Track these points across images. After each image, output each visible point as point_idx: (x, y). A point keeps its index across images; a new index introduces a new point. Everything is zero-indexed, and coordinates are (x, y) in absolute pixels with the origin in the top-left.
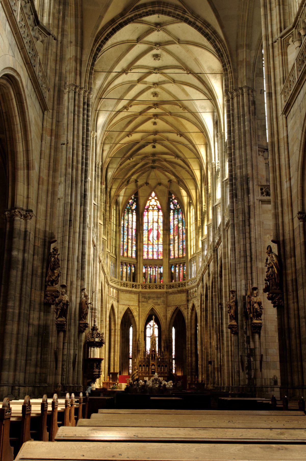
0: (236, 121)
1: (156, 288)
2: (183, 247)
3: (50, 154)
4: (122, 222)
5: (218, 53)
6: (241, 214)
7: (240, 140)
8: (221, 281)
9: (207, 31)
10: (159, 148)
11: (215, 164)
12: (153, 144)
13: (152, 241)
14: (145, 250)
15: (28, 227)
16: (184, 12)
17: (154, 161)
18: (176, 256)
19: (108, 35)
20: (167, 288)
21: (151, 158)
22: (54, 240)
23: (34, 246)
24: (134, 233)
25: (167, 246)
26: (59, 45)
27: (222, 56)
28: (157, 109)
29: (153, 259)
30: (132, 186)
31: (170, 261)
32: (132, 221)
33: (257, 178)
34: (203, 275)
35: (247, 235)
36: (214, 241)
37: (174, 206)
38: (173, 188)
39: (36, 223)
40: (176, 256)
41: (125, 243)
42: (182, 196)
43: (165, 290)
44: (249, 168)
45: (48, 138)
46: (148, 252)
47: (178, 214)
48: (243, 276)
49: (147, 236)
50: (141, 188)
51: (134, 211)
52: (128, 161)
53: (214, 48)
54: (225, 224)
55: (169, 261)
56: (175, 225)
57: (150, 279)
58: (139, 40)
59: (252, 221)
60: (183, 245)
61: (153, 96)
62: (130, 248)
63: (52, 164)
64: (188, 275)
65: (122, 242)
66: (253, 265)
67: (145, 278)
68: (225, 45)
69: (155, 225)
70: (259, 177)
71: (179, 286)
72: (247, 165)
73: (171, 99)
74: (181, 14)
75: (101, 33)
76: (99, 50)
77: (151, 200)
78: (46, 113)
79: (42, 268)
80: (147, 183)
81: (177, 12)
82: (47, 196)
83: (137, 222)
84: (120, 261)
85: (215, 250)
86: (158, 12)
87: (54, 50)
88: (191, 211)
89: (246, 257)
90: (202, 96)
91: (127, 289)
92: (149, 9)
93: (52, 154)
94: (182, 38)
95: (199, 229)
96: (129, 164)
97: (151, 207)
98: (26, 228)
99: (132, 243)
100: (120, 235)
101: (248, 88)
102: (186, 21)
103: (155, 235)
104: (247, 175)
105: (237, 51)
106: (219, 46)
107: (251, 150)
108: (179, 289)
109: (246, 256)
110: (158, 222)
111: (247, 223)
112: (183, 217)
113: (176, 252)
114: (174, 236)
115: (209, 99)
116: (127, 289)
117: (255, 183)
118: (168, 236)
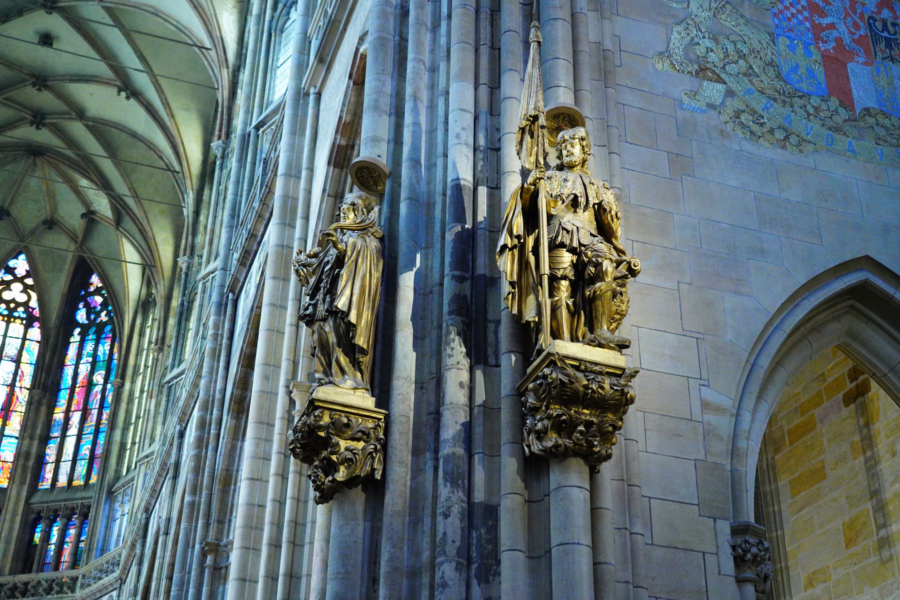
2: (93, 451)
8: (238, 434)
17: (39, 118)
18: (63, 480)
25: (36, 442)
31: (35, 499)
37: (88, 315)
38: (99, 245)
40: (63, 480)
47: (97, 342)
55: (29, 497)
56: (80, 378)
60: (94, 443)
88: (148, 331)
110: (17, 361)
112: (115, 350)
113: (65, 468)
114: (68, 412)
118: (43, 410)
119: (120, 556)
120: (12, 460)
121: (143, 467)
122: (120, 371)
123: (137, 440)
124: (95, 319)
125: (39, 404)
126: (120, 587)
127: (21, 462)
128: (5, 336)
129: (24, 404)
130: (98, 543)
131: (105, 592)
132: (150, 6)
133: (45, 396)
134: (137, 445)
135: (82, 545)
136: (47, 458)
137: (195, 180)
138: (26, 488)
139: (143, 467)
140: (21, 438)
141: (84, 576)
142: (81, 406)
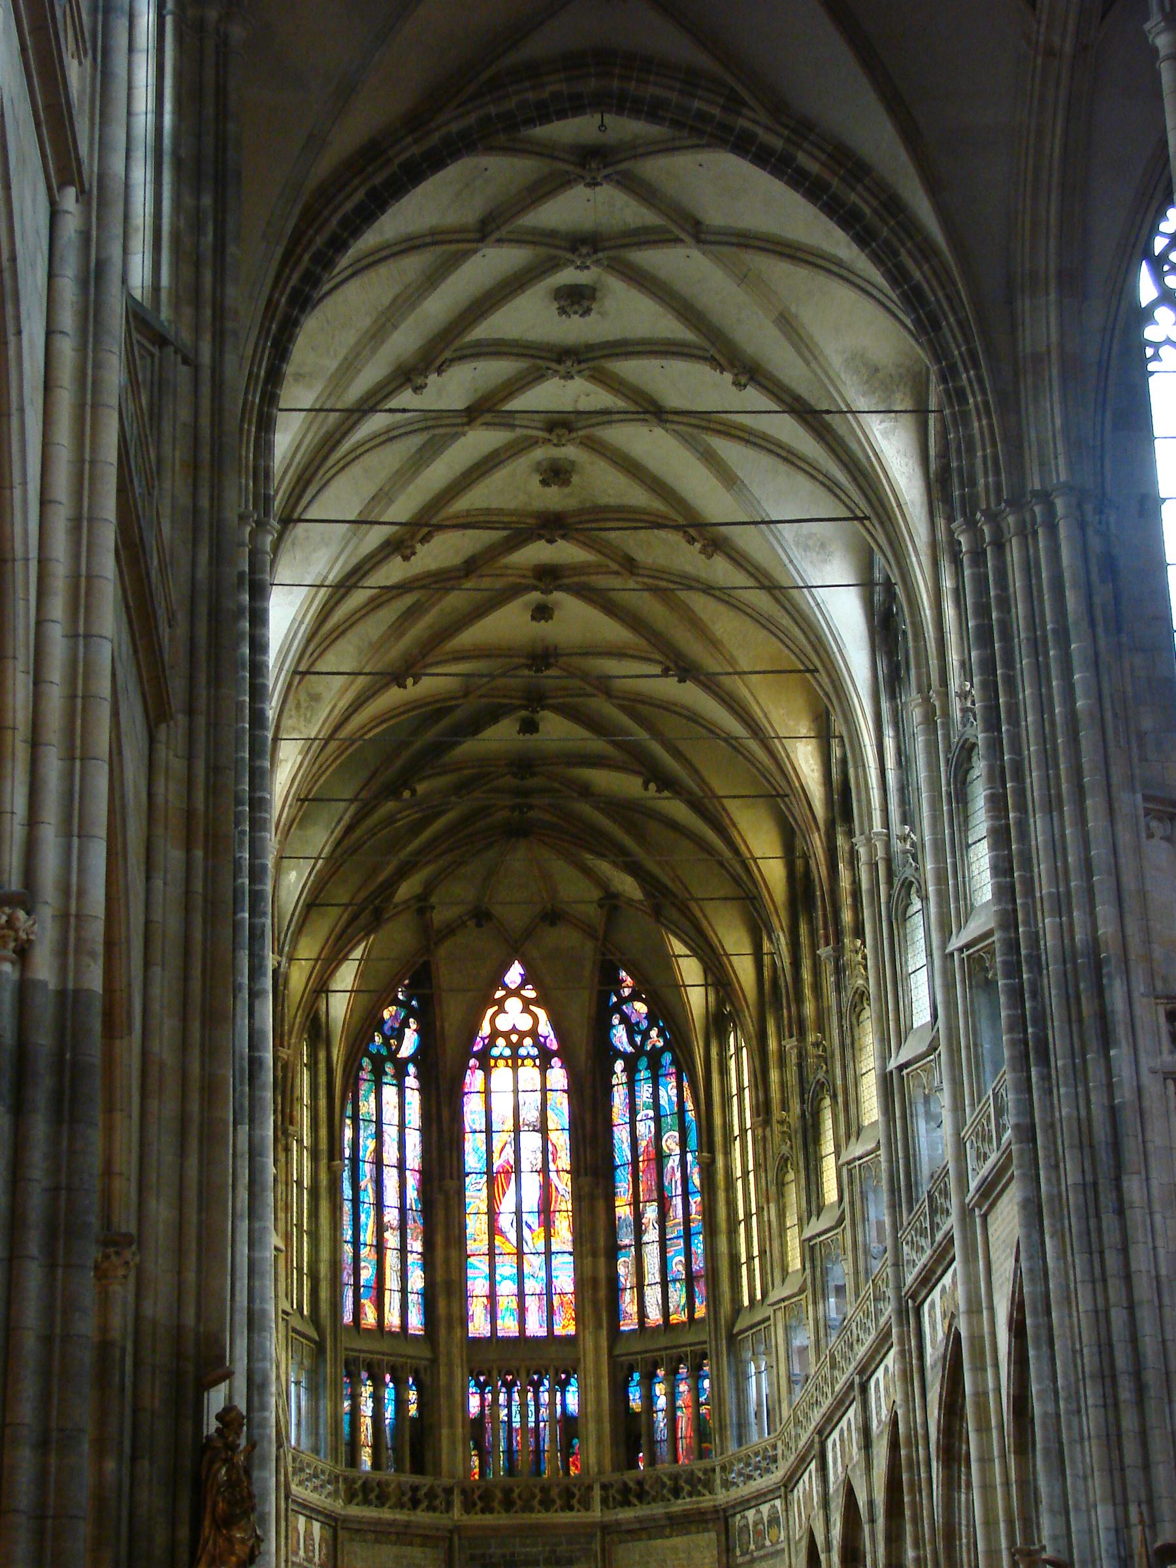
0: (1024, 662)
1: (547, 1504)
2: (688, 1265)
3: (187, 940)
4: (348, 1133)
5: (915, 310)
6: (1076, 1151)
7: (1049, 760)
9: (853, 197)
10: (556, 730)
11: (888, 845)
12: (523, 713)
13: (512, 1235)
14: (478, 1285)
15: (116, 1321)
16: (734, 103)
18: (654, 1315)
19: (345, 223)
20: (604, 1501)
21: (508, 781)
22: (220, 1371)
23: (135, 1411)
24: (412, 1194)
25: (602, 1260)
26: (206, 390)
27: (936, 327)
28: (560, 541)
29: (522, 1338)
30: (398, 936)
32: (402, 1126)
33: (1149, 958)
34: (823, 1432)
35: (1112, 1261)
36: (897, 1264)
39: (138, 1295)
40: (654, 1315)
41: (364, 1251)
42: (678, 987)
43: (596, 1514)
44: (1105, 910)
45: (175, 855)
46: (492, 1297)
48: (1098, 1485)
49: (484, 1208)
50: (448, 944)
51: (412, 1069)
52: (391, 805)
53: (894, 282)
54: (973, 1185)
57: (509, 1451)
58: (486, 229)
59: (1133, 1187)
61: (545, 483)
62: (392, 1281)
63: (196, 986)
64: (722, 1428)
65: (348, 1249)
66: (1152, 1419)
67: (479, 1446)
68: (947, 272)
69: (531, 1142)
70: (1158, 952)
71: (676, 1492)
72: (1090, 891)
73: (639, 497)
74: (716, 111)
75: (310, 217)
76: (303, 300)
77: (501, 1003)
78: (162, 732)
79: (173, 1524)
80: (481, 916)
81: (697, 104)
82: (182, 1154)
83: (424, 1130)
84: (342, 1355)
85: (910, 1309)
86: (601, 102)
87: (185, 414)
88: (732, 1064)
89: (1114, 1378)
90: (829, 507)
91: (386, 1514)
92: (555, 85)
93: (198, 936)
94: (715, 216)
95: (782, 1170)
96: (391, 819)
97: (501, 1042)
98: (104, 1329)
99: (403, 1251)
100: (336, 1209)
101: (1079, 496)
102: (744, 145)
103: (531, 1200)
104: (1095, 943)
105: (1010, 302)
106: (917, 275)
107: (1111, 811)
108: (680, 1505)
109: (1107, 1376)
111: (1107, 1199)
112: (687, 1093)
113: (653, 1295)
114: (635, 1202)
115: (856, 518)
116: (386, 1514)
117: (1140, 988)
118: (601, 1205)
119: (775, 1447)
120: (571, 1289)
121: (780, 1314)
122: (704, 1139)
123: (756, 1253)
124: (643, 1042)
125: (592, 1197)
126: (786, 1497)
127: (588, 1294)
128: (516, 1091)
129: (568, 1197)
130: (731, 1417)
131: (763, 1499)
132: (682, 706)
133: (597, 1185)
134: (757, 1261)
135: (703, 1410)
136: (622, 1280)
137: (783, 914)
138: (604, 1332)
139: (780, 1314)
140: (577, 1253)
141: (723, 1468)
142: (655, 1195)
